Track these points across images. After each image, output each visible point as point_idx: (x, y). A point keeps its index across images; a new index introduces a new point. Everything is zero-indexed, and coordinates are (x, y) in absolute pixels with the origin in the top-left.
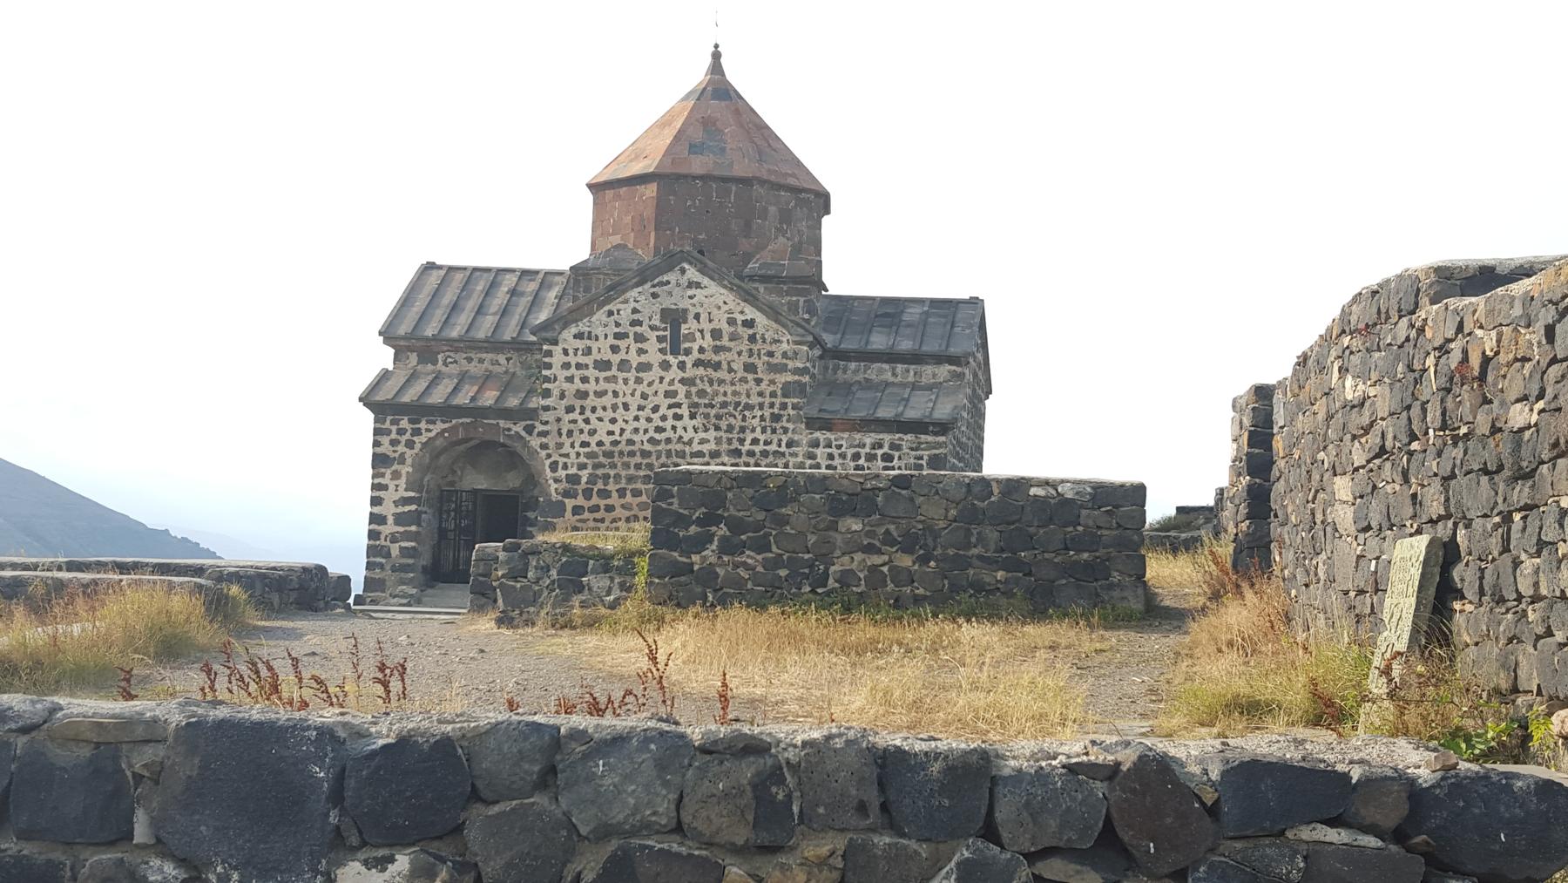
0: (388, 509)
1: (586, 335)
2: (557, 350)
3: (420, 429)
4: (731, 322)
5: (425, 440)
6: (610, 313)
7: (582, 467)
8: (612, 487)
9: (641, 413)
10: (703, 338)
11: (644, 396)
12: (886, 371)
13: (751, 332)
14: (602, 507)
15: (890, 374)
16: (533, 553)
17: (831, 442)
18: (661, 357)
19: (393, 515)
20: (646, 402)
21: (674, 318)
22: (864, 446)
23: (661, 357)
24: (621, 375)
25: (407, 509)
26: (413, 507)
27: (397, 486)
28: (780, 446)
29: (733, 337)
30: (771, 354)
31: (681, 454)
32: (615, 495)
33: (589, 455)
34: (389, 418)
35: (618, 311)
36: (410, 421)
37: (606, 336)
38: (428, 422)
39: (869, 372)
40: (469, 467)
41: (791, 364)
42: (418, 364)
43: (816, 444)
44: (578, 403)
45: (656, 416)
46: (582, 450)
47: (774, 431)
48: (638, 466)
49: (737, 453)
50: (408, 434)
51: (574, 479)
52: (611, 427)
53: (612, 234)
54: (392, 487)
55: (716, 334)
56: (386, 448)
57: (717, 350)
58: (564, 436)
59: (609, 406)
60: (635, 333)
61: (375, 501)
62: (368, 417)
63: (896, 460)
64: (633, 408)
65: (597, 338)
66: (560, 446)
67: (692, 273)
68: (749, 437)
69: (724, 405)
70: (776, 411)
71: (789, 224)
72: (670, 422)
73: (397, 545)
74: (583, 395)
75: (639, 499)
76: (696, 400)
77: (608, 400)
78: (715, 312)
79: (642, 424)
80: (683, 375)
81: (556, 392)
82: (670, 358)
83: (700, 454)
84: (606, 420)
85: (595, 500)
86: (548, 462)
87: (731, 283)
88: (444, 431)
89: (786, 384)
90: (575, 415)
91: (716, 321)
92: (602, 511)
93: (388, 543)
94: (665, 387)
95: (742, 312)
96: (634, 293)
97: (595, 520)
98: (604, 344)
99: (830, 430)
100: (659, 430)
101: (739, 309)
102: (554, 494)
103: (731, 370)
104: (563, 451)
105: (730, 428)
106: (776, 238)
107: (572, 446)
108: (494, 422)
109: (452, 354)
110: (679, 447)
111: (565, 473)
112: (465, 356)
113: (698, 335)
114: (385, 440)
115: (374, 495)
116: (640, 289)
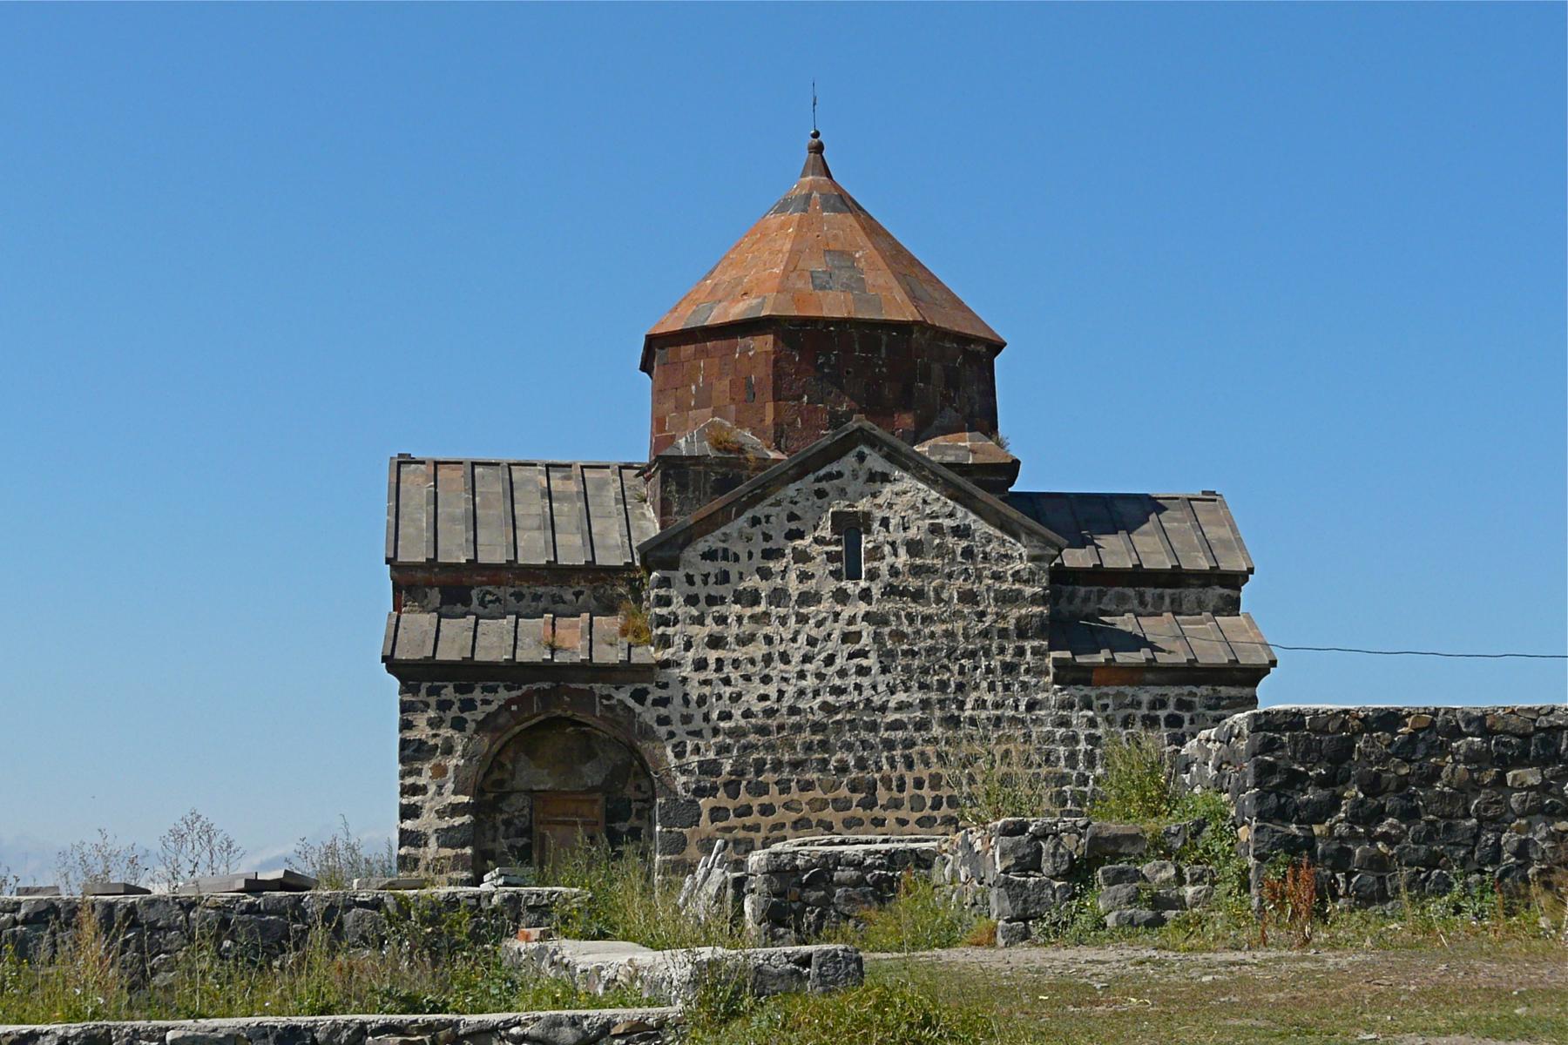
0: (427, 822)
1: (720, 554)
2: (679, 575)
3: (472, 701)
4: (935, 530)
5: (481, 717)
6: (755, 521)
7: (723, 750)
8: (768, 777)
9: (807, 666)
10: (896, 554)
11: (812, 642)
12: (1130, 597)
13: (964, 543)
14: (755, 809)
15: (1136, 602)
16: (1045, 837)
17: (1092, 702)
18: (833, 585)
19: (436, 831)
20: (816, 650)
22: (1139, 704)
23: (833, 585)
25: (458, 821)
26: (466, 819)
27: (440, 787)
28: (1017, 708)
29: (941, 551)
30: (997, 577)
31: (873, 727)
32: (774, 789)
33: (736, 733)
34: (425, 686)
35: (768, 517)
36: (457, 689)
37: (750, 555)
38: (484, 689)
39: (1105, 600)
40: (523, 757)
41: (1028, 591)
42: (441, 604)
44: (712, 656)
45: (831, 670)
47: (1007, 687)
48: (808, 747)
50: (455, 707)
51: (710, 768)
52: (763, 690)
53: (697, 407)
54: (432, 789)
55: (914, 548)
56: (422, 731)
58: (693, 704)
60: (794, 549)
61: (408, 812)
62: (395, 683)
63: (1186, 724)
64: (796, 658)
65: (737, 558)
66: (686, 719)
67: (876, 462)
69: (930, 651)
70: (1008, 659)
71: (956, 389)
72: (853, 679)
74: (716, 642)
75: (811, 794)
77: (758, 650)
79: (810, 682)
80: (868, 608)
81: (679, 641)
82: (849, 585)
83: (896, 726)
84: (756, 680)
85: (744, 798)
87: (933, 473)
88: (510, 702)
90: (710, 674)
94: (837, 630)
95: (951, 515)
96: (791, 490)
97: (744, 827)
99: (1087, 683)
100: (838, 691)
101: (947, 510)
104: (692, 727)
105: (943, 685)
106: (942, 408)
107: (706, 718)
108: (586, 687)
109: (490, 588)
111: (696, 758)
112: (512, 590)
113: (887, 549)
114: (421, 720)
115: (405, 801)
116: (798, 484)
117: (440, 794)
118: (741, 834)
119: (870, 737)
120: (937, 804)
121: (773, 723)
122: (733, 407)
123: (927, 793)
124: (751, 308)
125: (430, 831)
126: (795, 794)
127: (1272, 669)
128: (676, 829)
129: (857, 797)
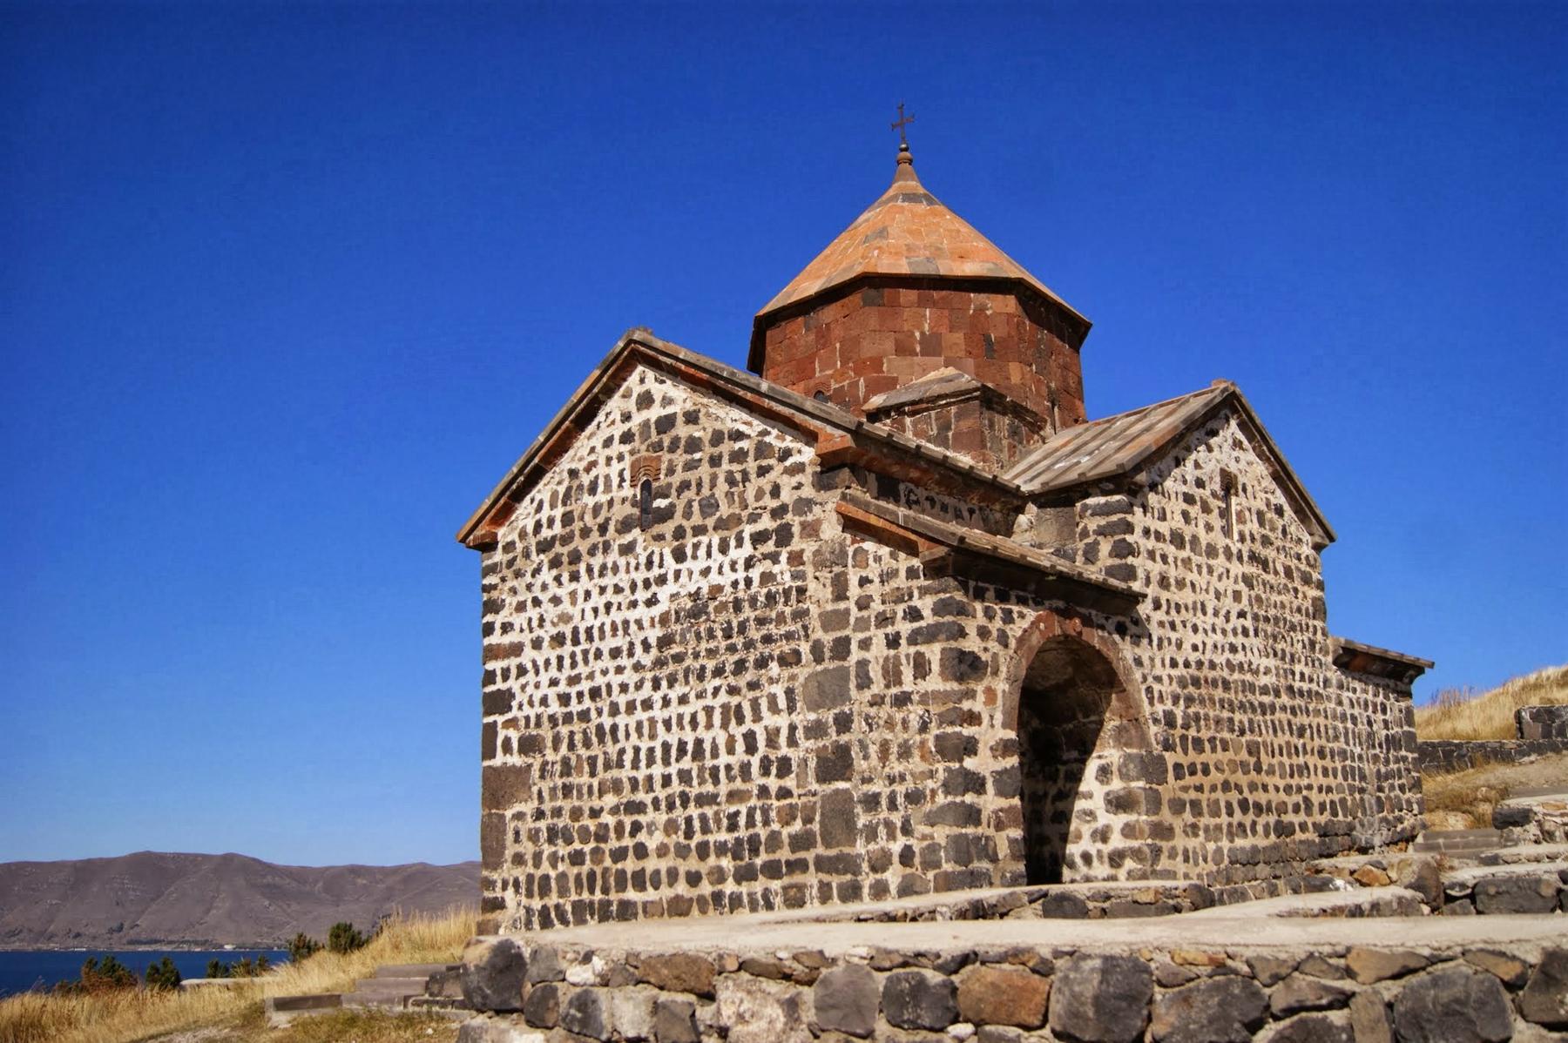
4: (1268, 505)
5: (1019, 633)
14: (1199, 767)
21: (1229, 484)
24: (1196, 559)
27: (992, 717)
30: (1299, 558)
32: (1207, 746)
33: (1182, 683)
34: (972, 584)
43: (1341, 687)
44: (1164, 596)
46: (1175, 672)
48: (1222, 701)
49: (1290, 689)
51: (1170, 721)
55: (1260, 515)
56: (972, 644)
57: (1266, 541)
59: (1190, 606)
66: (1152, 659)
68: (1298, 668)
69: (1276, 619)
73: (1004, 834)
74: (1164, 582)
76: (1256, 610)
77: (1186, 597)
78: (1257, 488)
82: (1228, 541)
83: (1265, 690)
86: (1143, 687)
89: (1315, 600)
91: (1259, 500)
92: (1200, 773)
93: (991, 832)
94: (1227, 585)
98: (1176, 507)
100: (1233, 649)
102: (1154, 743)
103: (1276, 573)
110: (1248, 677)
112: (925, 494)
113: (1247, 513)
117: (992, 726)
118: (1193, 795)
119: (1250, 696)
120: (1292, 776)
121: (1201, 675)
122: (970, 362)
123: (1285, 759)
124: (989, 269)
125: (987, 775)
126: (1220, 755)
127: (1427, 670)
128: (1154, 786)
129: (1252, 760)
